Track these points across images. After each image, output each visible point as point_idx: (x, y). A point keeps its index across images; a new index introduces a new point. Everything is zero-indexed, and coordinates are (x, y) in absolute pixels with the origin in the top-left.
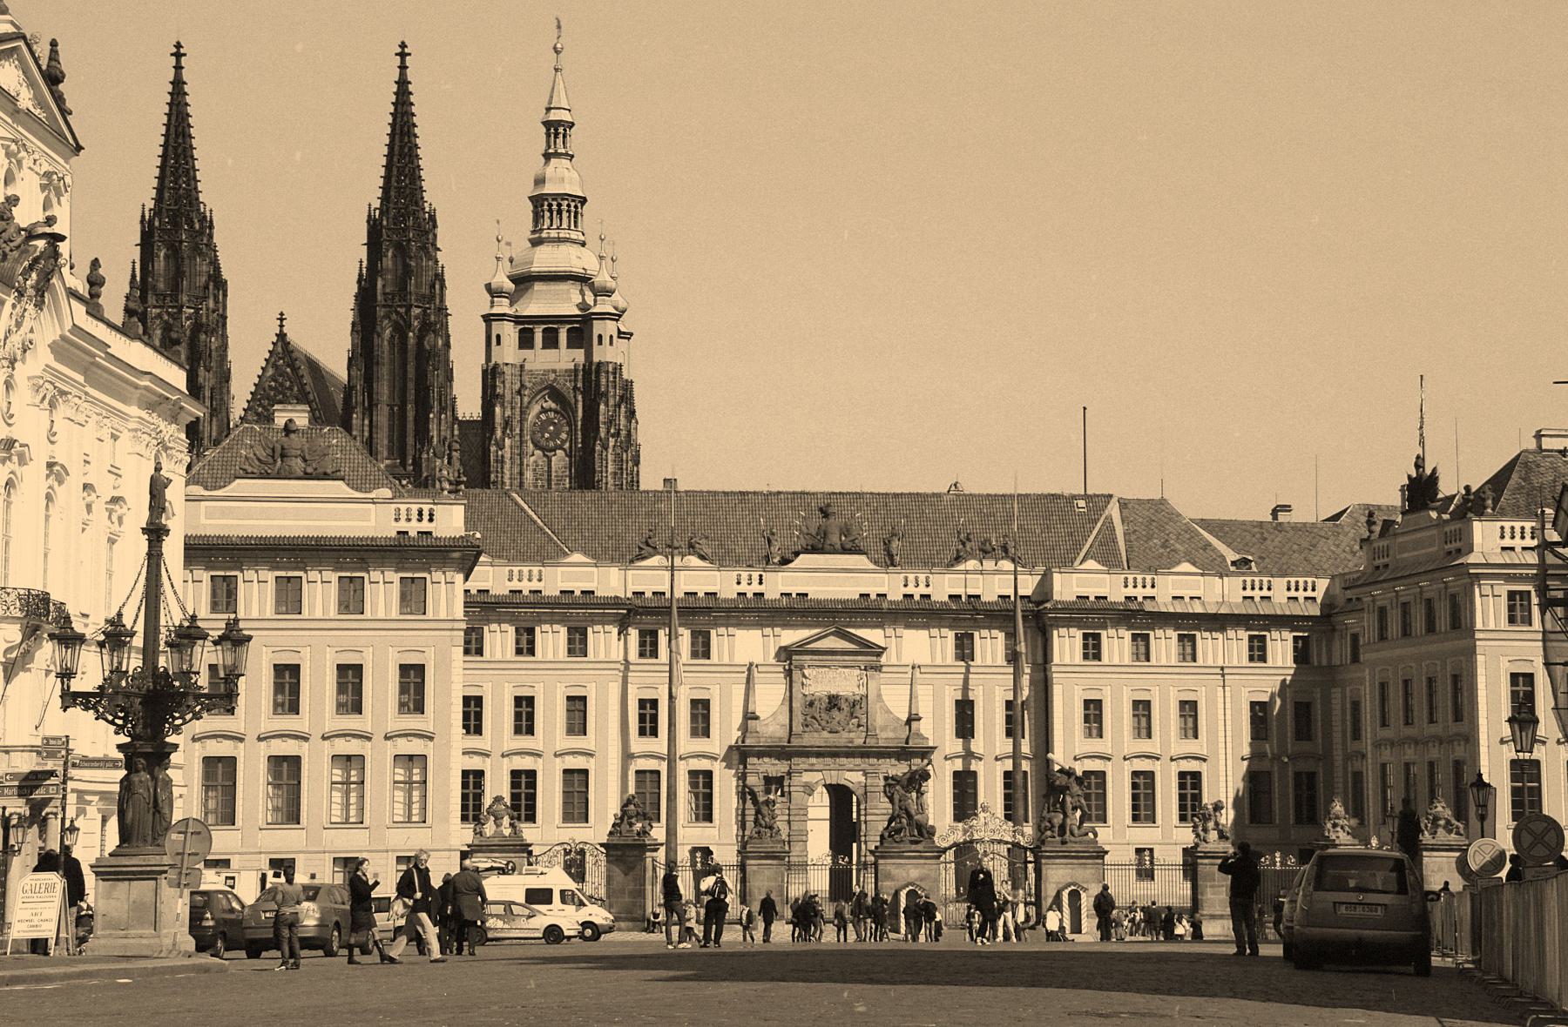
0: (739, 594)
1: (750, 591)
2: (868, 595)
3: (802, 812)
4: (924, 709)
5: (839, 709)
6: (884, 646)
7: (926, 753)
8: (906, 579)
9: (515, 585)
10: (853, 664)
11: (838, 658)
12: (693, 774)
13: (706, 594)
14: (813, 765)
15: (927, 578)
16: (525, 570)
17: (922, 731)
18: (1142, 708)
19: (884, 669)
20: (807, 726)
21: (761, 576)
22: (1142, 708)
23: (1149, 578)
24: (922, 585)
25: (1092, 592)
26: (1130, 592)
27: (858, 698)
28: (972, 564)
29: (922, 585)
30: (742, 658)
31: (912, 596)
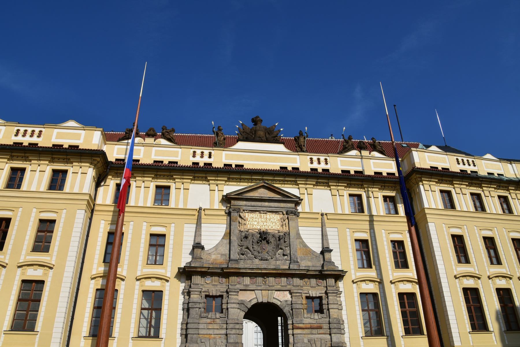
0: (194, 163)
2: (286, 168)
3: (237, 326)
5: (268, 242)
7: (339, 276)
8: (311, 159)
9: (19, 139)
10: (277, 210)
11: (266, 204)
12: (146, 293)
13: (170, 162)
14: (247, 285)
15: (326, 160)
17: (333, 260)
19: (301, 215)
20: (243, 254)
26: (461, 167)
27: (282, 234)
28: (354, 152)
30: (194, 205)
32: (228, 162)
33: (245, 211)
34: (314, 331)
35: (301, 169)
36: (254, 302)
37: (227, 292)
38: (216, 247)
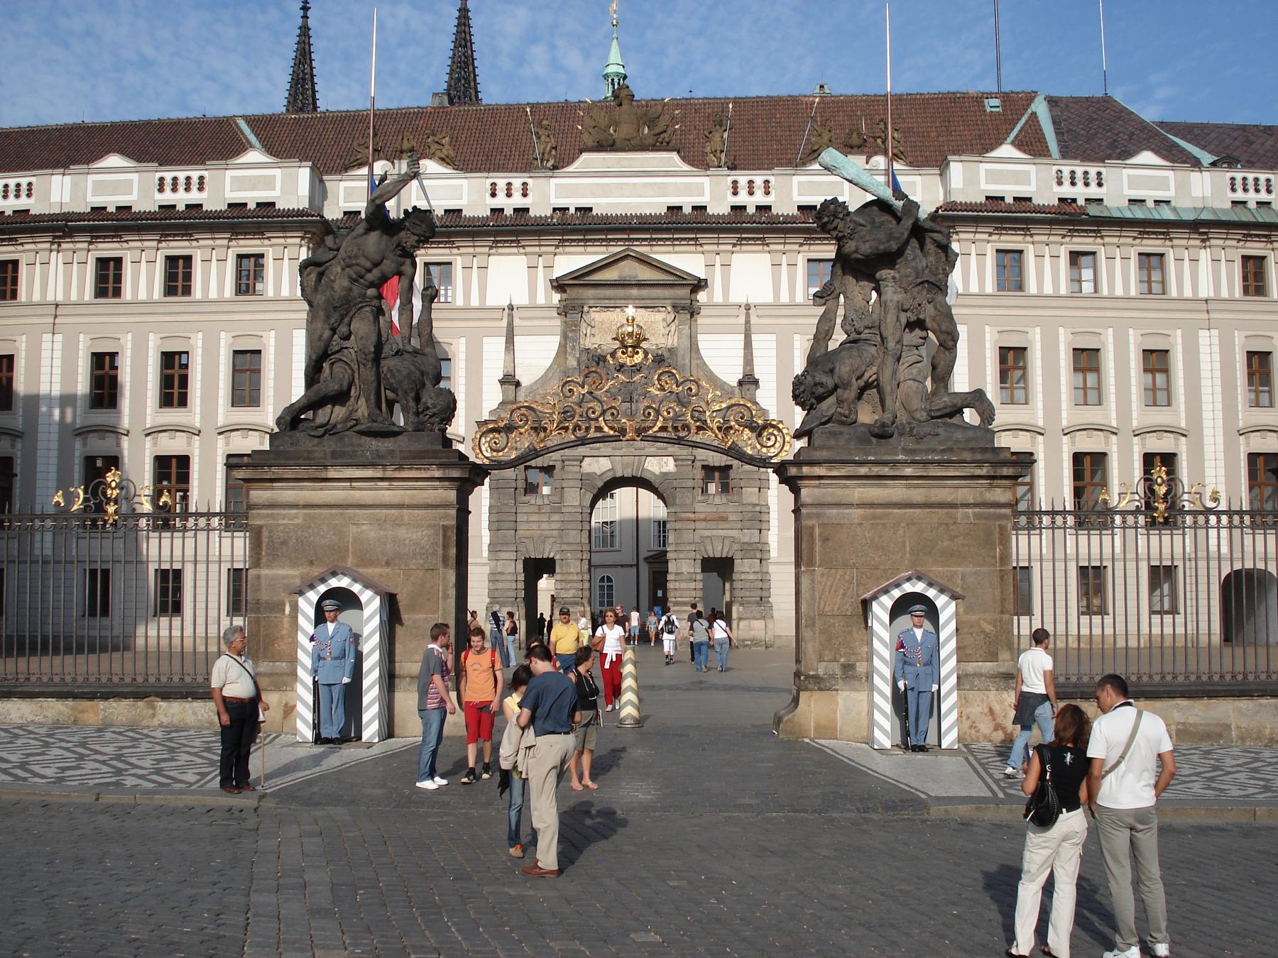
1: (508, 204)
2: (680, 208)
4: (765, 370)
6: (703, 277)
8: (735, 182)
9: (168, 197)
15: (767, 182)
16: (181, 176)
18: (1087, 360)
19: (703, 312)
21: (525, 184)
22: (1087, 360)
23: (1093, 171)
24: (759, 193)
25: (1009, 191)
26: (1066, 191)
29: (759, 193)
30: (497, 298)
31: (744, 208)
32: (561, 203)
33: (594, 309)
34: (713, 525)
35: (710, 211)
36: (609, 476)
37: (563, 461)
38: (544, 380)
